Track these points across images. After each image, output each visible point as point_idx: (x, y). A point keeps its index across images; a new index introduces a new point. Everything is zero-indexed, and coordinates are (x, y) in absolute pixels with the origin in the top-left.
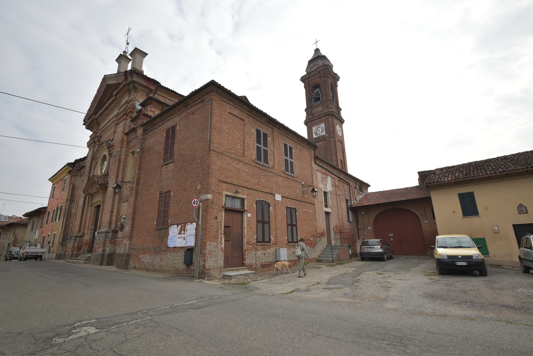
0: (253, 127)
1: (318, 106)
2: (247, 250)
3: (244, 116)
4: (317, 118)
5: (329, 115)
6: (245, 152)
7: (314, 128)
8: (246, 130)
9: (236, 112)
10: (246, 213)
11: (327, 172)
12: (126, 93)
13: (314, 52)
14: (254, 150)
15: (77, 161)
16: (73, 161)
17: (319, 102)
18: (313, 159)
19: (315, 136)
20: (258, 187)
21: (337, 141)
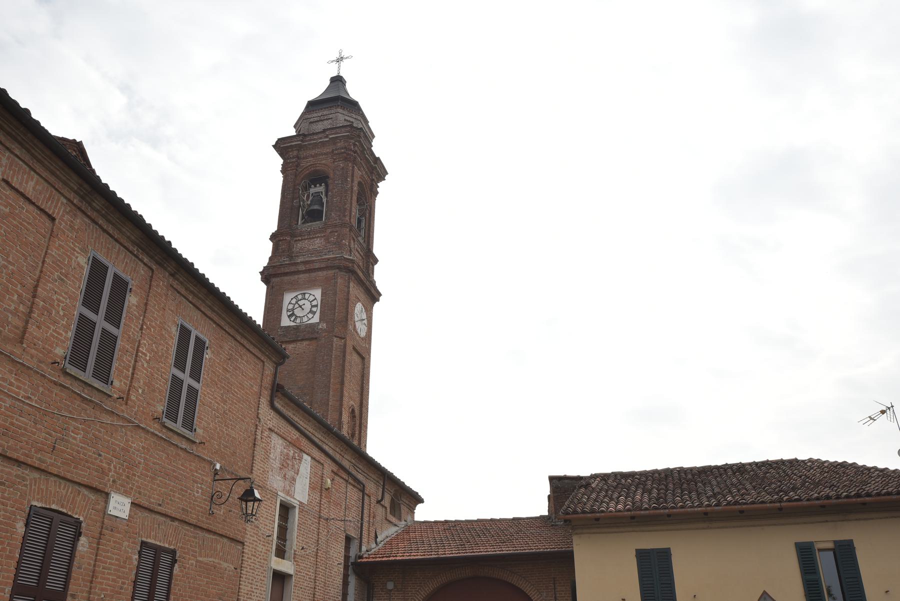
0: (84, 250)
1: (311, 235)
3: (59, 207)
5: (339, 268)
6: (32, 328)
7: (288, 298)
8: (53, 252)
9: (31, 185)
11: (304, 442)
13: (327, 83)
14: (67, 328)
17: (316, 225)
18: (266, 393)
19: (286, 322)
20: (49, 461)
21: (349, 349)
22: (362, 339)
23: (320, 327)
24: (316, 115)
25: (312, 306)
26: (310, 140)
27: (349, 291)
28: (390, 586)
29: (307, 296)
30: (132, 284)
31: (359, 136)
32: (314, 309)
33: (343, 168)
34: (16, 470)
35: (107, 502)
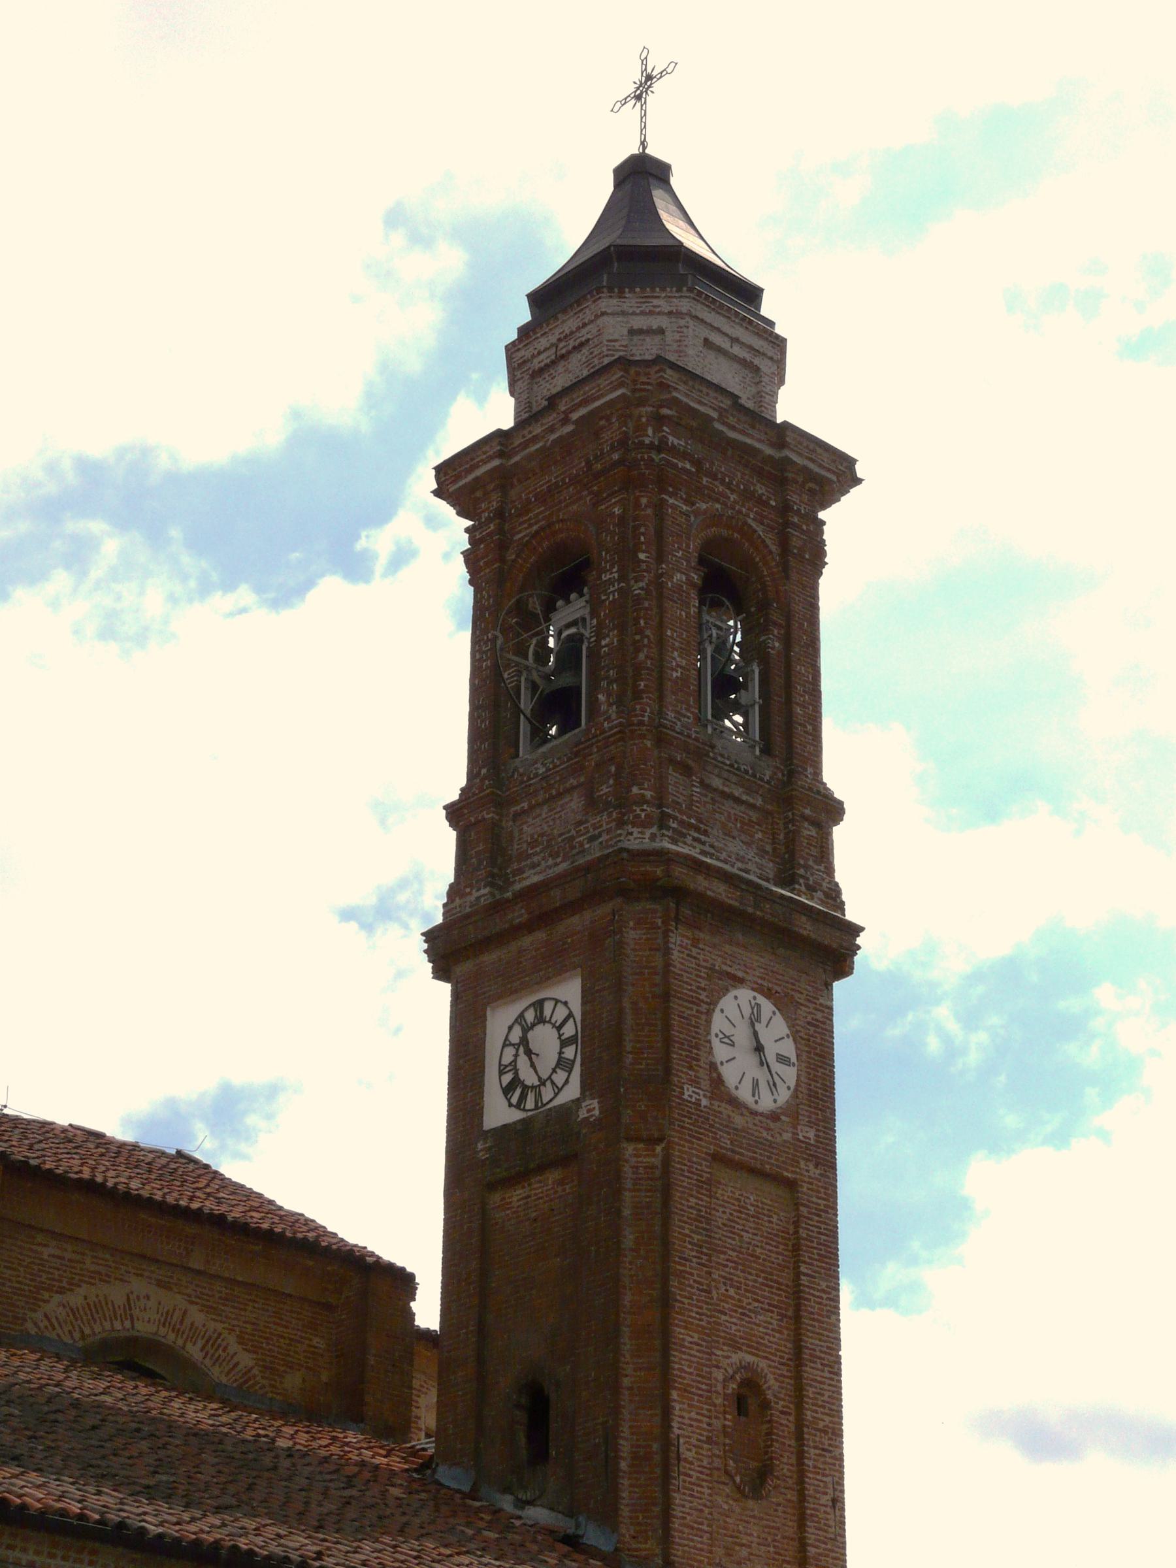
4: (519, 915)
5: (624, 892)
7: (500, 1022)
22: (774, 1116)
23: (583, 1114)
24: (543, 343)
25: (564, 1043)
26: (525, 445)
27: (668, 965)
29: (548, 1007)
31: (663, 386)
32: (569, 1052)
33: (622, 519)
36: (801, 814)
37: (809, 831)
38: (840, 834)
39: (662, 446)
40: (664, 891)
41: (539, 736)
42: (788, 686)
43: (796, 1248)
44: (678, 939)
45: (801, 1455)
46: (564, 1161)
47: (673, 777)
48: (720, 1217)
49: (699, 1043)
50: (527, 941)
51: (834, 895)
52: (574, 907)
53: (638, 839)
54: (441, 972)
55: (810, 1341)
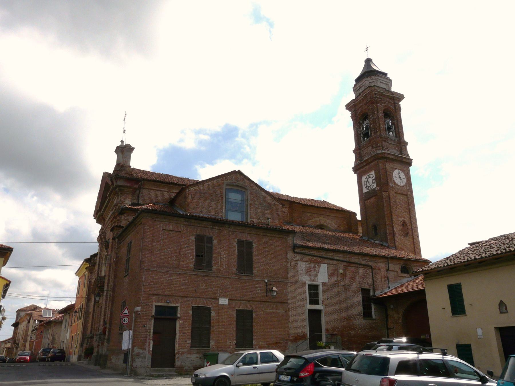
2: (178, 354)
4: (364, 164)
7: (364, 178)
10: (179, 319)
11: (319, 259)
12: (115, 195)
14: (192, 258)
15: (92, 256)
16: (89, 257)
22: (403, 186)
28: (392, 306)
30: (214, 237)
31: (375, 89)
34: (187, 299)
35: (219, 301)
36: (402, 145)
37: (403, 147)
38: (408, 147)
39: (376, 97)
40: (384, 158)
41: (364, 140)
42: (398, 127)
43: (408, 204)
44: (387, 164)
45: (412, 231)
46: (375, 196)
47: (384, 142)
48: (397, 201)
49: (391, 178)
50: (366, 167)
51: (408, 155)
52: (372, 162)
53: (380, 151)
54: (355, 173)
55: (412, 216)
